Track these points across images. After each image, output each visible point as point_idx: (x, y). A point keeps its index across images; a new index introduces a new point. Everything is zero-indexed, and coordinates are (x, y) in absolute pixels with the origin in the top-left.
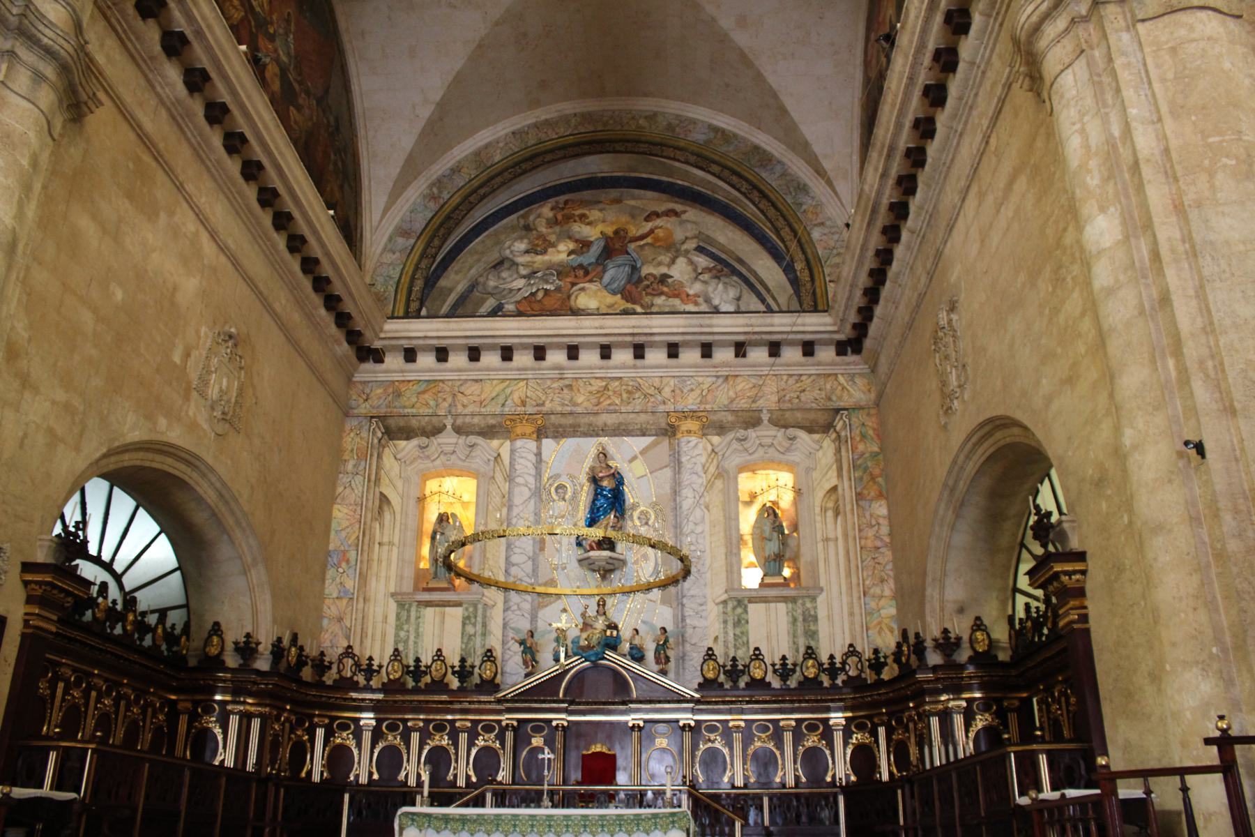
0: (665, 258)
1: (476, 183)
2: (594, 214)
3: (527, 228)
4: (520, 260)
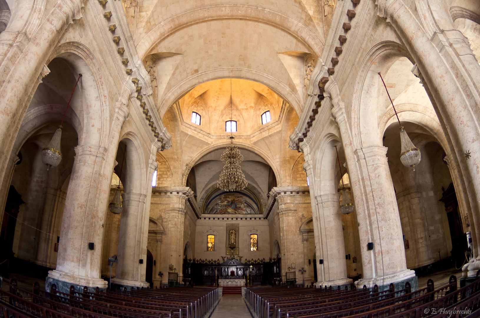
0: (240, 204)
1: (212, 191)
2: (230, 197)
3: (220, 199)
4: (220, 204)
